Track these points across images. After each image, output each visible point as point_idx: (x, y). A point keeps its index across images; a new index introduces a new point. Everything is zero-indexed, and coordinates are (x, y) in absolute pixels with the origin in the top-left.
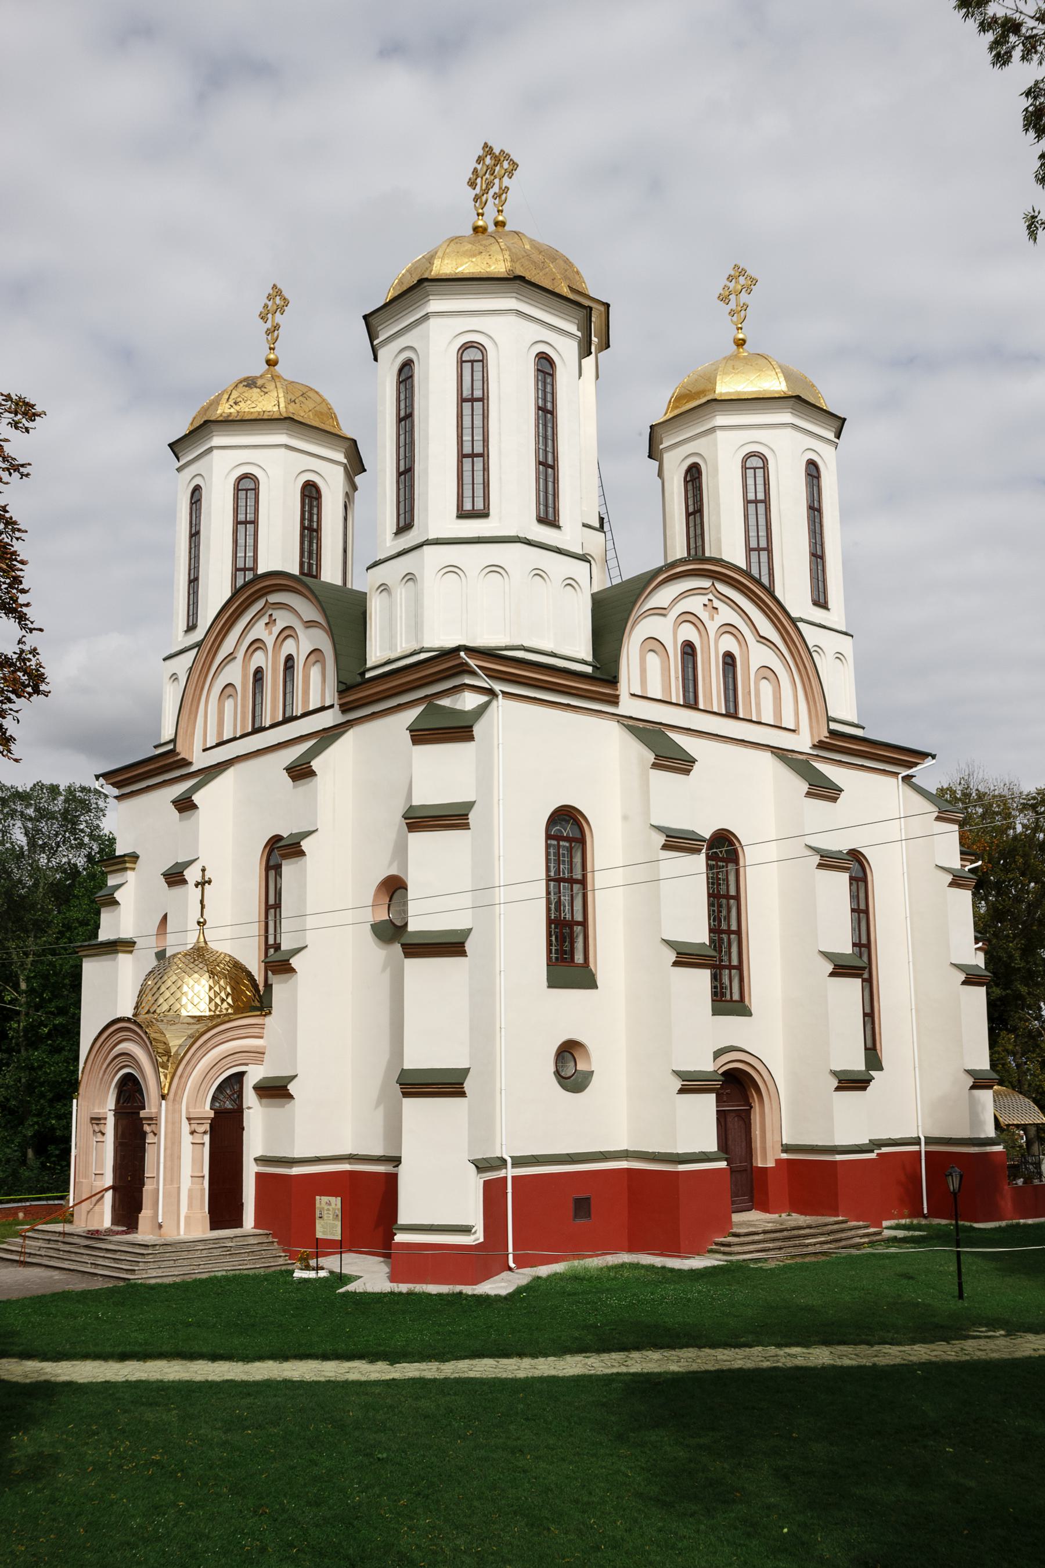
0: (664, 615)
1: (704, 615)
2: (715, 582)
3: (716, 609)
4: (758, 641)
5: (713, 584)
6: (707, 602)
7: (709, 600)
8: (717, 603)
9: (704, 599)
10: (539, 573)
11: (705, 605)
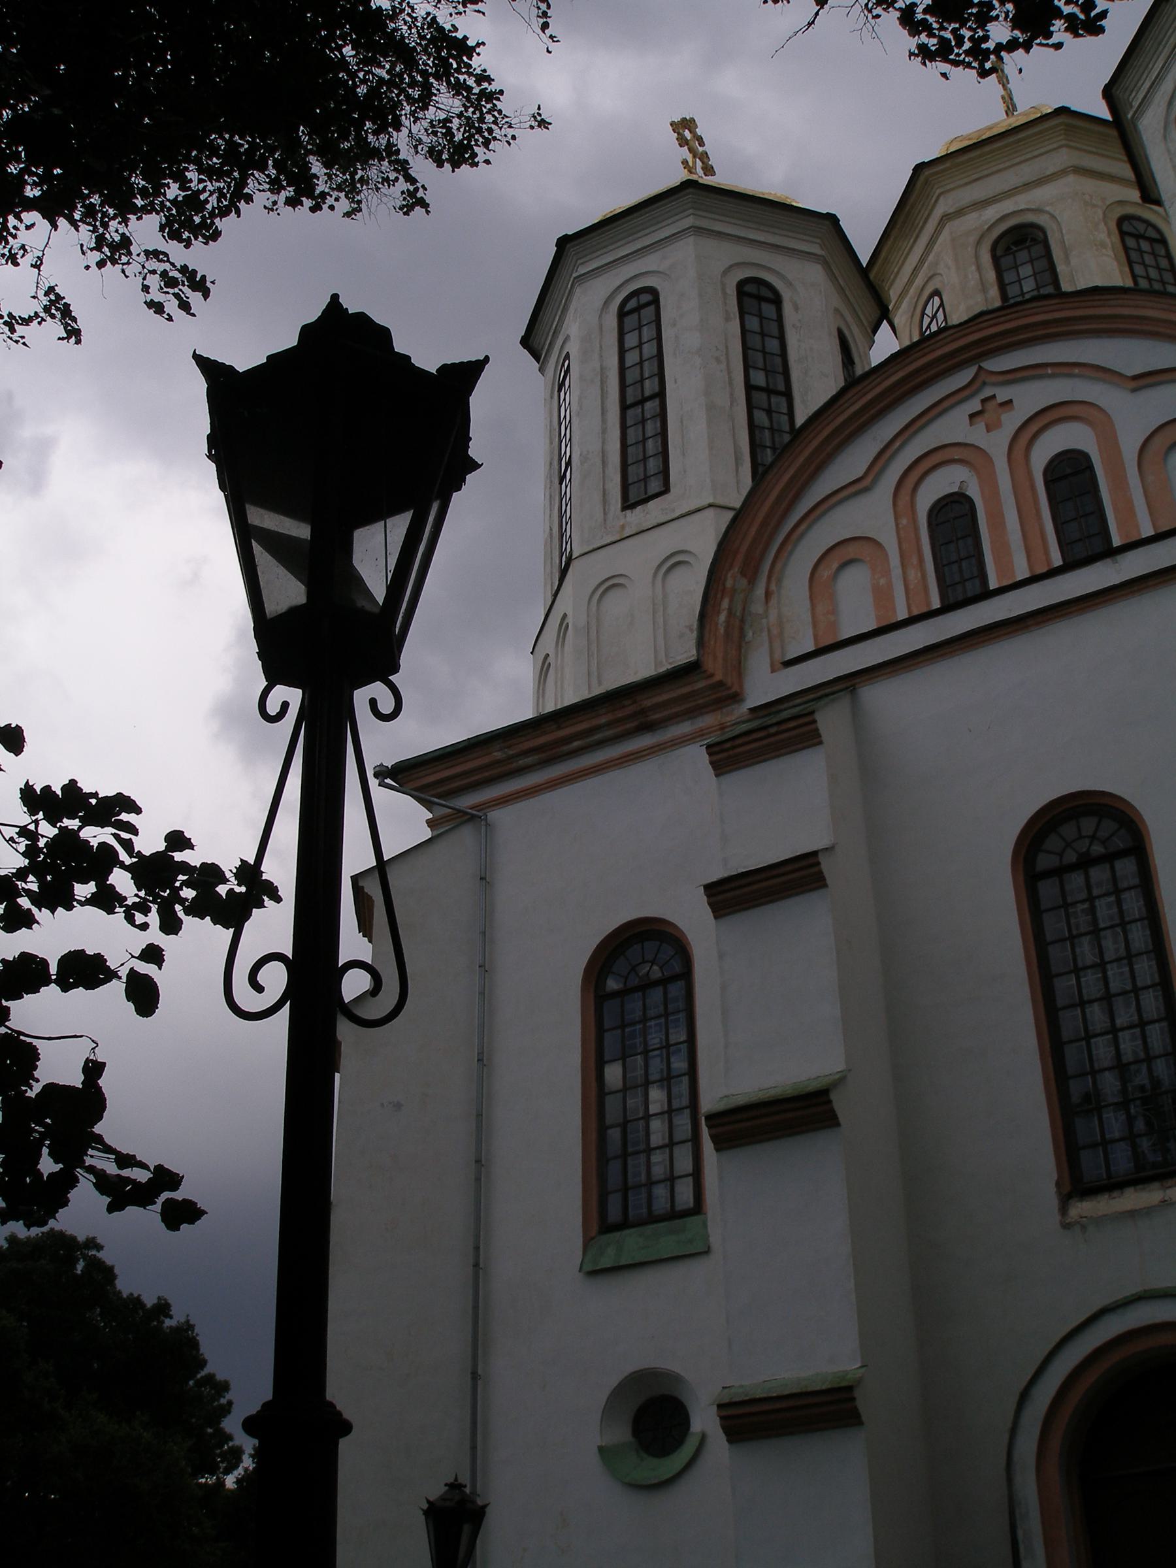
0: (867, 489)
1: (977, 435)
2: (982, 364)
3: (1010, 401)
4: (1134, 390)
5: (980, 368)
6: (979, 408)
7: (984, 401)
8: (1002, 394)
9: (975, 405)
10: (611, 585)
11: (972, 416)
